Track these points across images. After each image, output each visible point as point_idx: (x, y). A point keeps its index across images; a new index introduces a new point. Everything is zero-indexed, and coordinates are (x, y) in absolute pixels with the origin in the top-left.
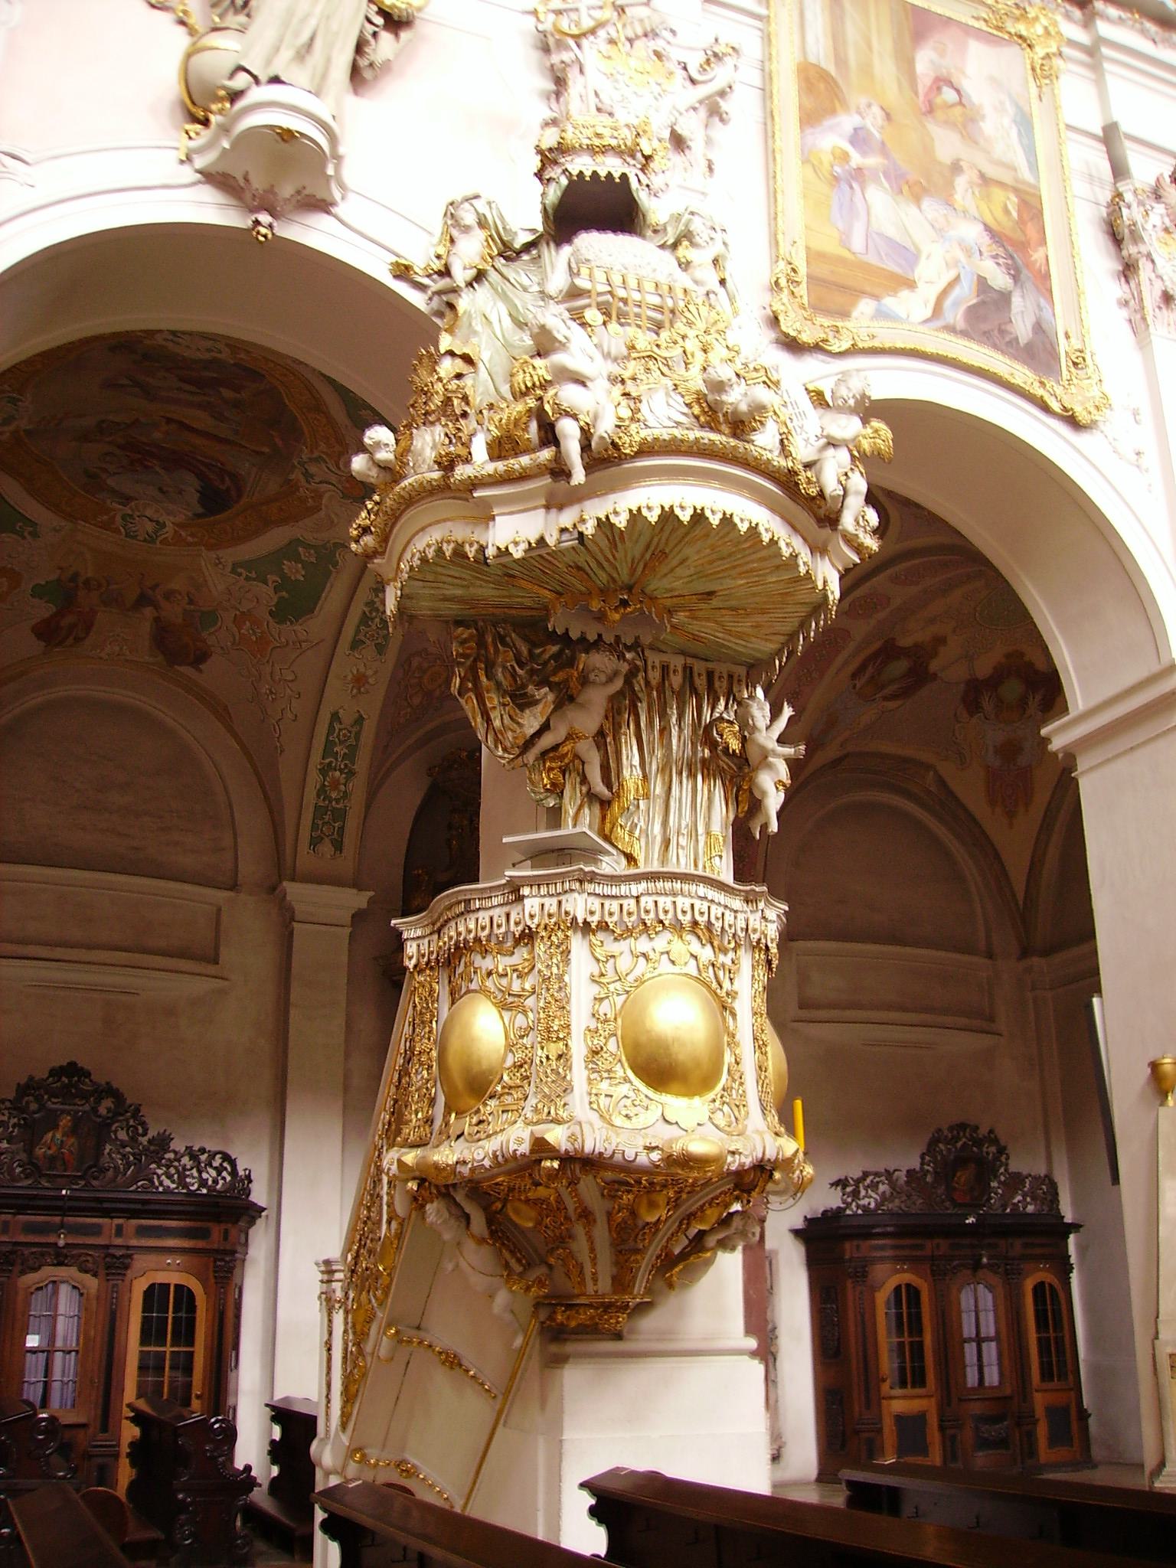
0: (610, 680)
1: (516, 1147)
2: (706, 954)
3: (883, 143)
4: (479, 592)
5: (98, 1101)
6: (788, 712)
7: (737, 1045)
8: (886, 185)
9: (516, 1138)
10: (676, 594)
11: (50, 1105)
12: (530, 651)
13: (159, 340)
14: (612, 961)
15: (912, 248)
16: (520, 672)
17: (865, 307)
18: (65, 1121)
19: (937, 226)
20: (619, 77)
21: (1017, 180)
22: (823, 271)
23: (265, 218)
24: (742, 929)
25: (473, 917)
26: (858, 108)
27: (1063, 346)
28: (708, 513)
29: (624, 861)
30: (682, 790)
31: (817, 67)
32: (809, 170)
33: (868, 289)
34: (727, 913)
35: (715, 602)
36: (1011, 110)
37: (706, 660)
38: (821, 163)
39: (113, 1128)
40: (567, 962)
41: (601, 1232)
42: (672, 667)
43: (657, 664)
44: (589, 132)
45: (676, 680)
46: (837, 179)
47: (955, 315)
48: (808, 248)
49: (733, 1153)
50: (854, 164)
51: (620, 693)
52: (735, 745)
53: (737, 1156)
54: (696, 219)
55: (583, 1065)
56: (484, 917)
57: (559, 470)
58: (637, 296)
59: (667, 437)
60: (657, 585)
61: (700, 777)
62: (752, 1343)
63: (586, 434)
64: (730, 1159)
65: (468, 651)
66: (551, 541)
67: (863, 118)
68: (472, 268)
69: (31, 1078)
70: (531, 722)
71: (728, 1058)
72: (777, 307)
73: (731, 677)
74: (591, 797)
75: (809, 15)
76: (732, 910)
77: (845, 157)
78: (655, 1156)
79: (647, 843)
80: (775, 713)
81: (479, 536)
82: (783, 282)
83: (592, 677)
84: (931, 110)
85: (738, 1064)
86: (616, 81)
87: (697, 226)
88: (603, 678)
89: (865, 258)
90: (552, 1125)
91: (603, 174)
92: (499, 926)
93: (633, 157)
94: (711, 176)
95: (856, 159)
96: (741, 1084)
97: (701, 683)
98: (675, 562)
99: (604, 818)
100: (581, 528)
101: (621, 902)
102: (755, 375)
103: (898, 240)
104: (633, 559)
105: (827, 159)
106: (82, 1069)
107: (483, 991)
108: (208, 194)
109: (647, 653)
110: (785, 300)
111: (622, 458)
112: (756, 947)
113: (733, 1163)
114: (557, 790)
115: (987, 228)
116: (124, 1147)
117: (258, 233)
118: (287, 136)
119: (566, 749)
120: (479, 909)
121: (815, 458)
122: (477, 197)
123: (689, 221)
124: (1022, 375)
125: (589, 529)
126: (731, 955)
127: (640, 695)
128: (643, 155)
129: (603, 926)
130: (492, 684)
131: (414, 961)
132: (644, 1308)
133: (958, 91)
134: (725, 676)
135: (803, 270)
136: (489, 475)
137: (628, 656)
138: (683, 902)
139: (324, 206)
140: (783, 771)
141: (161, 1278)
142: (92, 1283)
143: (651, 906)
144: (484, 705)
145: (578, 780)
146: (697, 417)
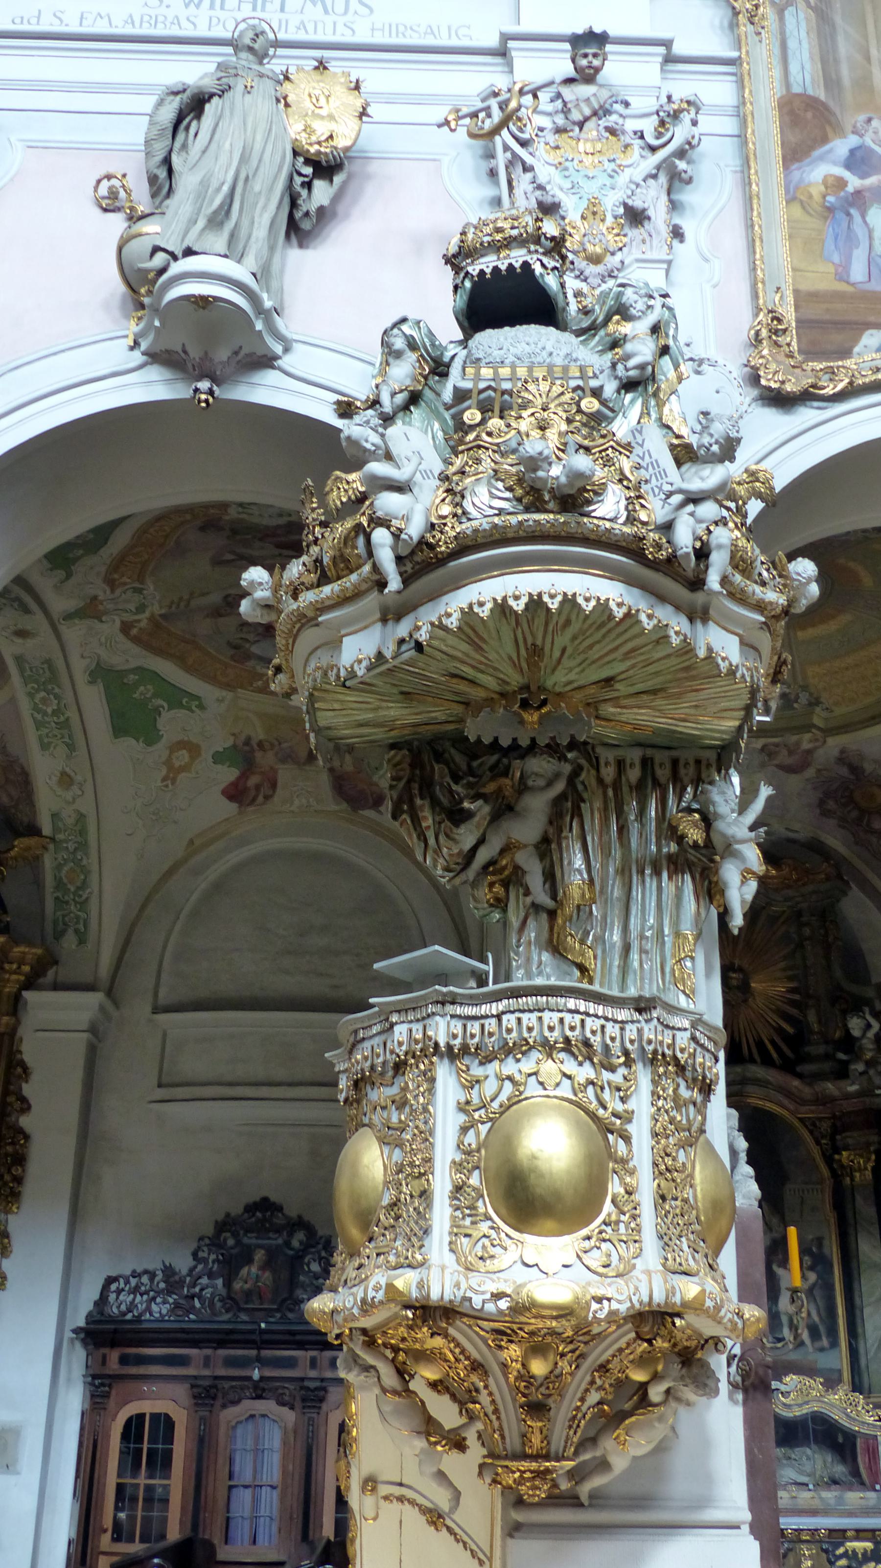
0: (550, 784)
1: (374, 1294)
2: (586, 1072)
4: (392, 713)
5: (291, 1235)
7: (632, 1172)
10: (575, 685)
11: (246, 1240)
12: (469, 766)
13: (233, 513)
14: (477, 1087)
16: (454, 787)
18: (259, 1256)
20: (568, 164)
22: (815, 312)
23: (204, 385)
24: (632, 1042)
25: (360, 1046)
26: (854, 127)
28: (546, 598)
29: (577, 973)
32: (797, 211)
33: (872, 319)
34: (609, 1026)
35: (622, 688)
37: (669, 748)
38: (811, 197)
39: (306, 1260)
40: (431, 1091)
42: (628, 762)
43: (611, 759)
44: (488, 230)
45: (634, 774)
46: (830, 210)
48: (796, 292)
49: (599, 1300)
50: (850, 189)
53: (605, 1302)
54: (629, 292)
55: (447, 1201)
59: (486, 526)
60: (558, 680)
61: (665, 875)
64: (594, 1306)
65: (402, 773)
66: (388, 654)
67: (861, 136)
68: (401, 391)
69: (228, 1215)
70: (467, 836)
71: (615, 1187)
73: (698, 762)
75: (792, 44)
76: (615, 1021)
77: (841, 183)
78: (503, 1304)
79: (604, 951)
82: (764, 333)
83: (530, 783)
85: (629, 1193)
86: (566, 169)
87: (629, 295)
88: (541, 782)
90: (408, 1270)
91: (503, 267)
92: (378, 1056)
93: (538, 242)
94: (682, 241)
95: (854, 182)
96: (634, 1217)
97: (663, 774)
98: (557, 654)
99: (551, 929)
100: (416, 636)
101: (482, 1021)
102: (602, 441)
104: (510, 658)
105: (816, 191)
106: (274, 1204)
107: (370, 1125)
108: (155, 373)
109: (599, 750)
110: (765, 352)
111: (443, 560)
112: (653, 1060)
113: (602, 1311)
114: (501, 904)
116: (317, 1279)
117: (199, 401)
118: (203, 302)
119: (504, 862)
120: (363, 1039)
121: (672, 517)
122: (404, 320)
123: (620, 295)
125: (423, 636)
126: (622, 1071)
127: (585, 796)
128: (546, 238)
130: (427, 803)
131: (344, 1095)
134: (692, 762)
135: (789, 314)
136: (328, 597)
137: (570, 755)
139: (267, 361)
140: (752, 856)
142: (289, 1416)
143: (513, 1024)
144: (421, 826)
145: (521, 891)
146: (519, 500)
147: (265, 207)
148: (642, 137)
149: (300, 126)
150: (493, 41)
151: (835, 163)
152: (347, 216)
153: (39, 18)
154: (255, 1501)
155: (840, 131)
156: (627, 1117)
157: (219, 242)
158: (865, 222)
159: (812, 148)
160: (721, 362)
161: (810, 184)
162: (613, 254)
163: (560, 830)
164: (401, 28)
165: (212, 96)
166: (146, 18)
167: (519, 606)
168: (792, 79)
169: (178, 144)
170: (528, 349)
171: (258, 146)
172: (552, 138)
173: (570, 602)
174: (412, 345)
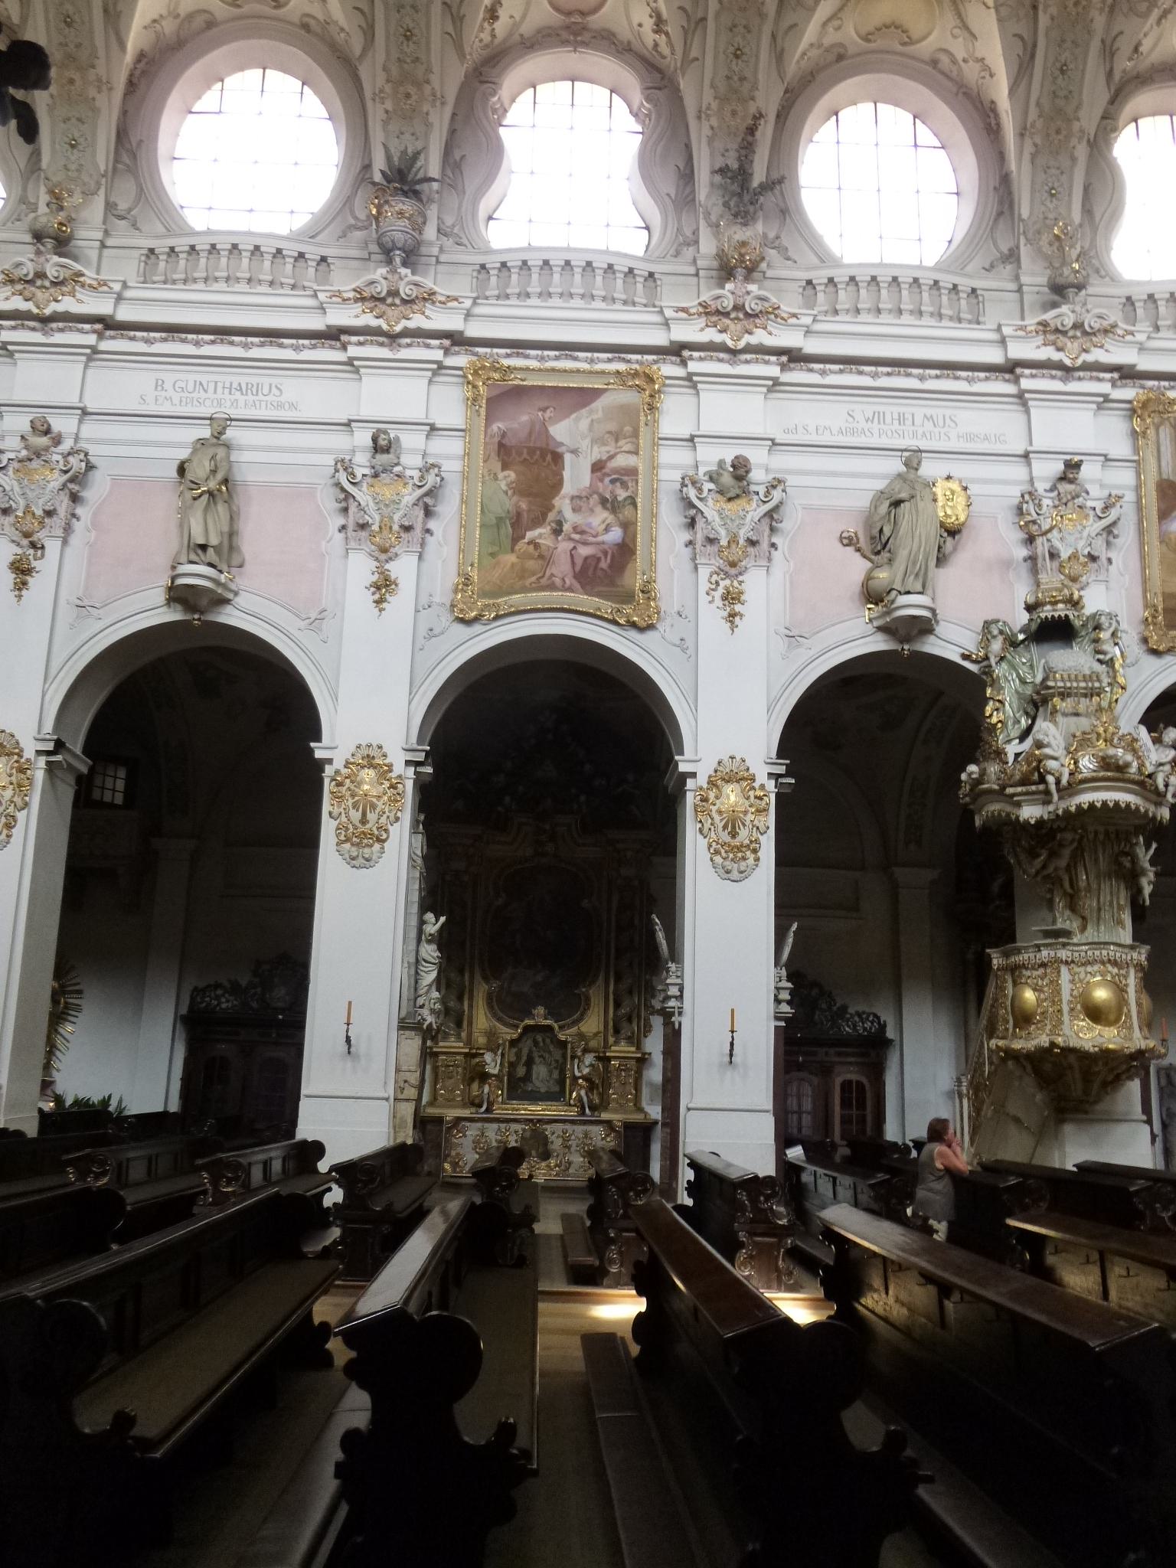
2: (1115, 970)
6: (1154, 846)
9: (1044, 1040)
30: (1106, 887)
31: (1168, 480)
32: (1165, 549)
41: (1077, 1075)
45: (1101, 837)
48: (1163, 593)
51: (1077, 848)
52: (1128, 865)
56: (1026, 956)
57: (1047, 792)
58: (1075, 684)
62: (1144, 1118)
63: (1058, 782)
72: (1147, 633)
74: (1065, 894)
75: (1163, 449)
78: (1097, 1049)
80: (1148, 848)
81: (1015, 811)
108: (880, 636)
114: (1051, 891)
129: (1073, 962)
132: (1096, 1102)
138: (1104, 952)
140: (1151, 876)
141: (849, 1077)
142: (816, 1080)
148: (1094, 509)
154: (800, 1119)
156: (1126, 985)
163: (1076, 864)
167: (1099, 805)
173: (1117, 804)
174: (1001, 632)
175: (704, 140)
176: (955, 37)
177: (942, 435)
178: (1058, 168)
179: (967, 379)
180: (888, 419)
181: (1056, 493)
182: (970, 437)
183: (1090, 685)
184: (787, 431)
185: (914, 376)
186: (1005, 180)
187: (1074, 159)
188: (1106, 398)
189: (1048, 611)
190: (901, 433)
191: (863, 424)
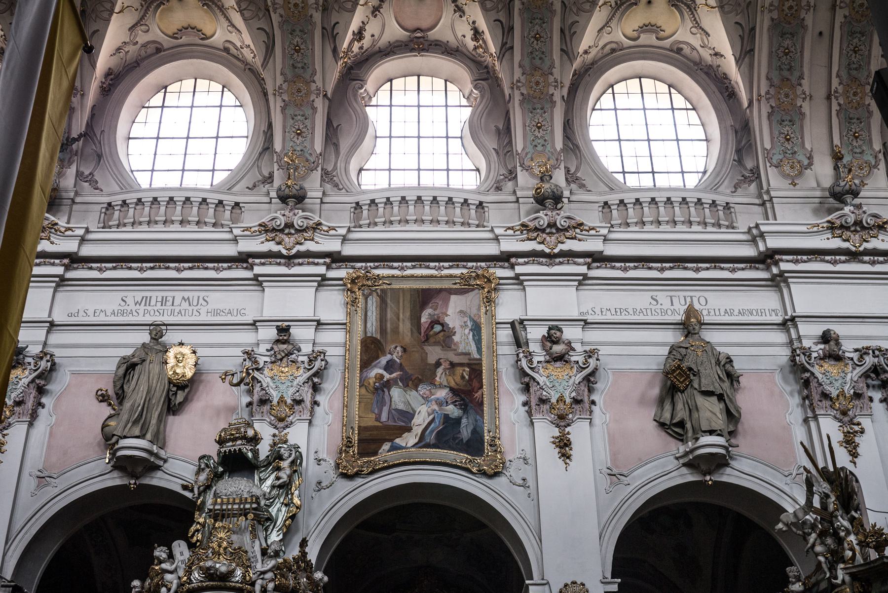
3: (401, 364)
8: (401, 384)
15: (411, 412)
17: (386, 446)
19: (425, 396)
21: (470, 360)
22: (366, 435)
26: (390, 351)
27: (487, 438)
32: (363, 391)
33: (387, 437)
36: (469, 324)
38: (369, 384)
46: (376, 389)
47: (431, 438)
48: (359, 427)
50: (385, 379)
75: (369, 314)
77: (382, 376)
84: (427, 339)
86: (274, 379)
89: (387, 423)
95: (387, 376)
103: (404, 409)
105: (371, 381)
108: (116, 474)
115: (452, 390)
117: (131, 488)
124: (461, 457)
133: (442, 325)
147: (156, 409)
149: (171, 373)
150: (251, 322)
151: (380, 368)
152: (192, 400)
153: (78, 313)
155: (384, 354)
157: (137, 431)
158: (389, 394)
159: (372, 361)
160: (328, 460)
161: (369, 378)
162: (289, 417)
164: (219, 311)
165: (137, 365)
166: (120, 311)
168: (367, 330)
169: (126, 381)
170: (235, 489)
171: (154, 385)
172: (270, 366)
175: (278, 109)
176: (230, 32)
177: (195, 311)
178: (303, 116)
179: (213, 269)
180: (153, 302)
181: (272, 352)
182: (216, 313)
183: (242, 506)
184: (70, 315)
185: (618, 269)
186: (270, 126)
187: (315, 109)
188: (324, 278)
189: (228, 447)
190: (161, 312)
191: (132, 307)
